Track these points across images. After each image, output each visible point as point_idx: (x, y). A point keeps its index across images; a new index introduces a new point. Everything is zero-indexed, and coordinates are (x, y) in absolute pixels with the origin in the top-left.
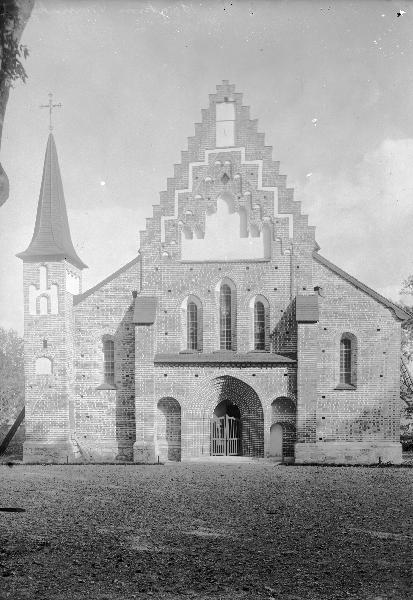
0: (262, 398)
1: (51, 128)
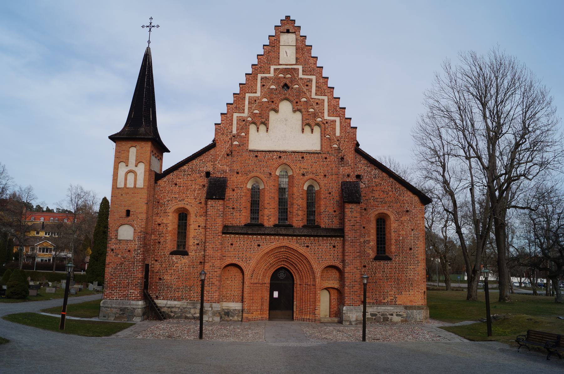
0: (315, 266)
1: (149, 42)
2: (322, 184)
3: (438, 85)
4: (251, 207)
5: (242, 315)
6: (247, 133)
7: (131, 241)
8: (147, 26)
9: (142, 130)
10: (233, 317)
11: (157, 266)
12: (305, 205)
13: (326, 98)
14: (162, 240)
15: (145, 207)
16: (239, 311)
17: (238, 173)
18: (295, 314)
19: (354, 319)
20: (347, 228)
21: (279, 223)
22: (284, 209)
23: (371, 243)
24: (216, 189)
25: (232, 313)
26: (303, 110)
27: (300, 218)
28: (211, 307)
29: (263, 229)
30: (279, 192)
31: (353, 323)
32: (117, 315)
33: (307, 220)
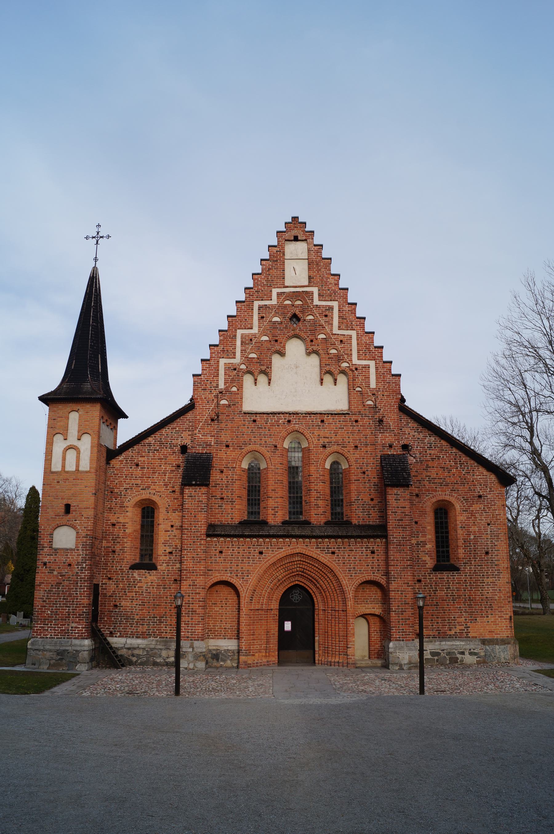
0: (345, 582)
1: (96, 259)
2: (352, 459)
3: (517, 310)
4: (249, 495)
5: (239, 659)
6: (240, 388)
7: (71, 550)
8: (93, 237)
9: (87, 386)
10: (224, 661)
11: (111, 586)
12: (328, 491)
13: (353, 333)
14: (118, 548)
15: (92, 499)
16: (233, 652)
17: (227, 446)
18: (317, 655)
19: (406, 661)
20: (391, 525)
21: (290, 518)
22: (297, 497)
23: (428, 546)
24: (197, 471)
25: (223, 655)
26: (321, 352)
27: (321, 510)
28: (192, 646)
29: (266, 528)
30: (290, 472)
31: (405, 668)
32: (52, 662)
33: (332, 514)
